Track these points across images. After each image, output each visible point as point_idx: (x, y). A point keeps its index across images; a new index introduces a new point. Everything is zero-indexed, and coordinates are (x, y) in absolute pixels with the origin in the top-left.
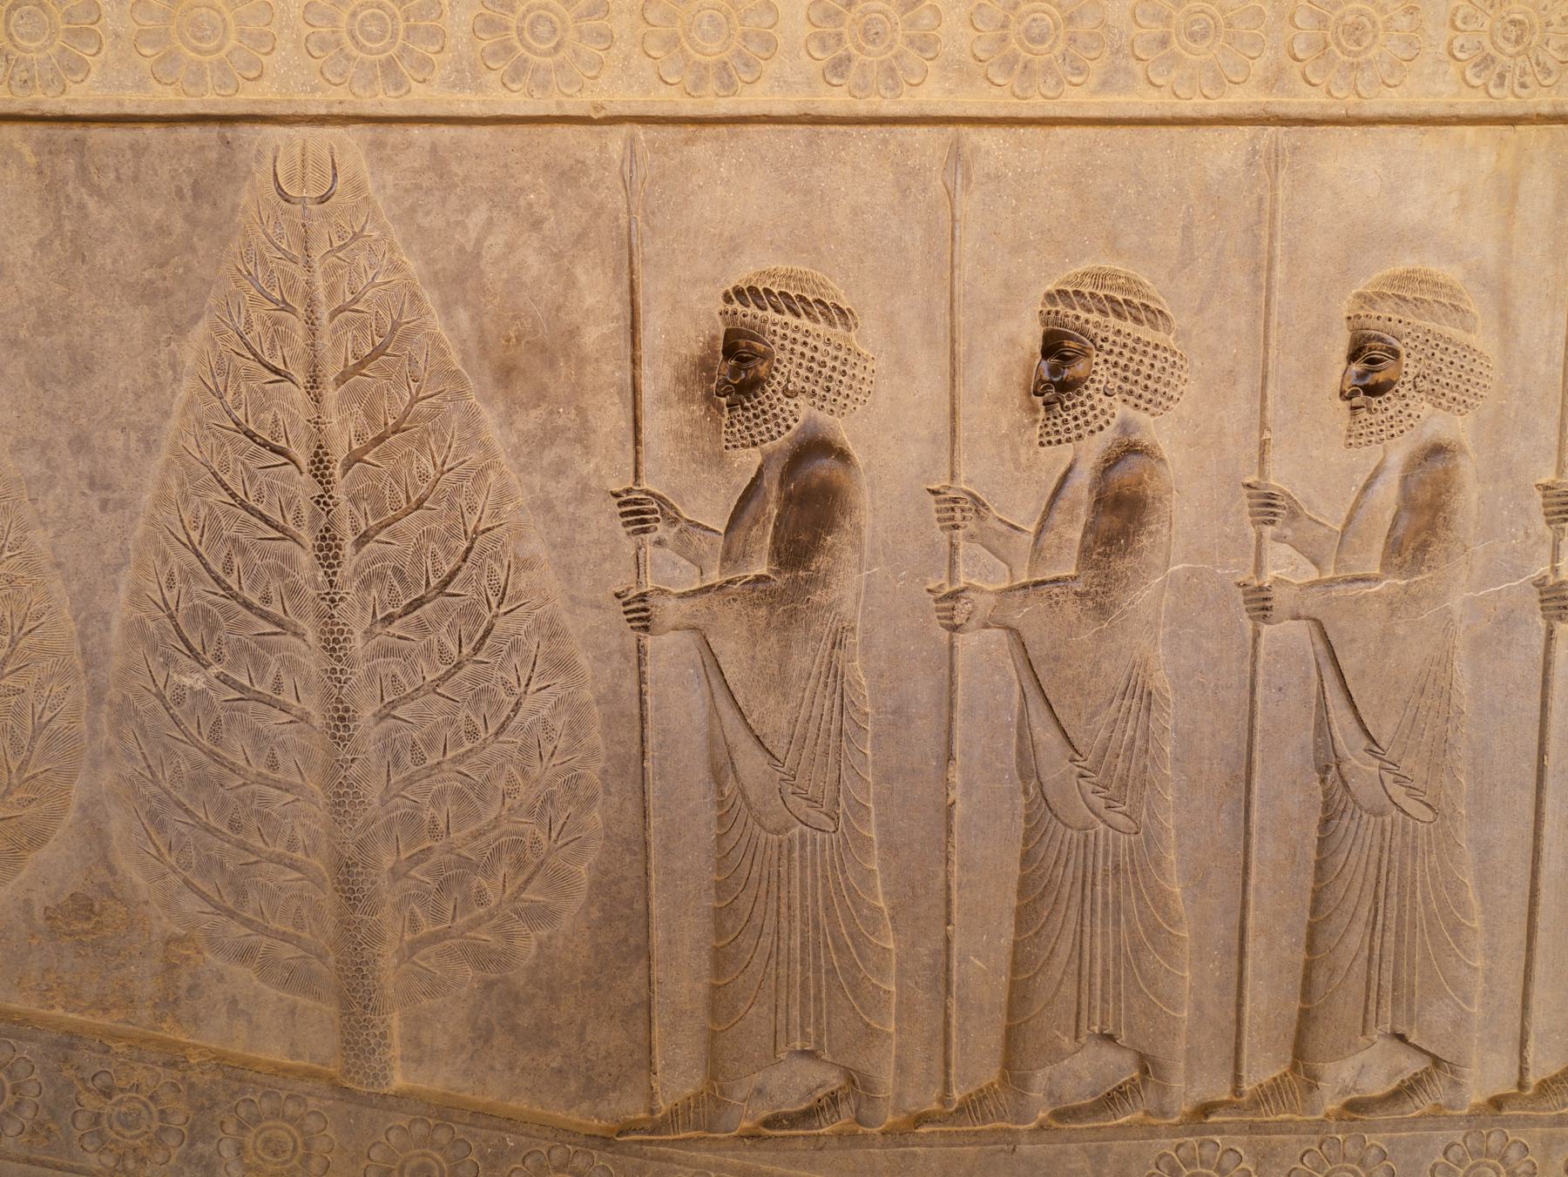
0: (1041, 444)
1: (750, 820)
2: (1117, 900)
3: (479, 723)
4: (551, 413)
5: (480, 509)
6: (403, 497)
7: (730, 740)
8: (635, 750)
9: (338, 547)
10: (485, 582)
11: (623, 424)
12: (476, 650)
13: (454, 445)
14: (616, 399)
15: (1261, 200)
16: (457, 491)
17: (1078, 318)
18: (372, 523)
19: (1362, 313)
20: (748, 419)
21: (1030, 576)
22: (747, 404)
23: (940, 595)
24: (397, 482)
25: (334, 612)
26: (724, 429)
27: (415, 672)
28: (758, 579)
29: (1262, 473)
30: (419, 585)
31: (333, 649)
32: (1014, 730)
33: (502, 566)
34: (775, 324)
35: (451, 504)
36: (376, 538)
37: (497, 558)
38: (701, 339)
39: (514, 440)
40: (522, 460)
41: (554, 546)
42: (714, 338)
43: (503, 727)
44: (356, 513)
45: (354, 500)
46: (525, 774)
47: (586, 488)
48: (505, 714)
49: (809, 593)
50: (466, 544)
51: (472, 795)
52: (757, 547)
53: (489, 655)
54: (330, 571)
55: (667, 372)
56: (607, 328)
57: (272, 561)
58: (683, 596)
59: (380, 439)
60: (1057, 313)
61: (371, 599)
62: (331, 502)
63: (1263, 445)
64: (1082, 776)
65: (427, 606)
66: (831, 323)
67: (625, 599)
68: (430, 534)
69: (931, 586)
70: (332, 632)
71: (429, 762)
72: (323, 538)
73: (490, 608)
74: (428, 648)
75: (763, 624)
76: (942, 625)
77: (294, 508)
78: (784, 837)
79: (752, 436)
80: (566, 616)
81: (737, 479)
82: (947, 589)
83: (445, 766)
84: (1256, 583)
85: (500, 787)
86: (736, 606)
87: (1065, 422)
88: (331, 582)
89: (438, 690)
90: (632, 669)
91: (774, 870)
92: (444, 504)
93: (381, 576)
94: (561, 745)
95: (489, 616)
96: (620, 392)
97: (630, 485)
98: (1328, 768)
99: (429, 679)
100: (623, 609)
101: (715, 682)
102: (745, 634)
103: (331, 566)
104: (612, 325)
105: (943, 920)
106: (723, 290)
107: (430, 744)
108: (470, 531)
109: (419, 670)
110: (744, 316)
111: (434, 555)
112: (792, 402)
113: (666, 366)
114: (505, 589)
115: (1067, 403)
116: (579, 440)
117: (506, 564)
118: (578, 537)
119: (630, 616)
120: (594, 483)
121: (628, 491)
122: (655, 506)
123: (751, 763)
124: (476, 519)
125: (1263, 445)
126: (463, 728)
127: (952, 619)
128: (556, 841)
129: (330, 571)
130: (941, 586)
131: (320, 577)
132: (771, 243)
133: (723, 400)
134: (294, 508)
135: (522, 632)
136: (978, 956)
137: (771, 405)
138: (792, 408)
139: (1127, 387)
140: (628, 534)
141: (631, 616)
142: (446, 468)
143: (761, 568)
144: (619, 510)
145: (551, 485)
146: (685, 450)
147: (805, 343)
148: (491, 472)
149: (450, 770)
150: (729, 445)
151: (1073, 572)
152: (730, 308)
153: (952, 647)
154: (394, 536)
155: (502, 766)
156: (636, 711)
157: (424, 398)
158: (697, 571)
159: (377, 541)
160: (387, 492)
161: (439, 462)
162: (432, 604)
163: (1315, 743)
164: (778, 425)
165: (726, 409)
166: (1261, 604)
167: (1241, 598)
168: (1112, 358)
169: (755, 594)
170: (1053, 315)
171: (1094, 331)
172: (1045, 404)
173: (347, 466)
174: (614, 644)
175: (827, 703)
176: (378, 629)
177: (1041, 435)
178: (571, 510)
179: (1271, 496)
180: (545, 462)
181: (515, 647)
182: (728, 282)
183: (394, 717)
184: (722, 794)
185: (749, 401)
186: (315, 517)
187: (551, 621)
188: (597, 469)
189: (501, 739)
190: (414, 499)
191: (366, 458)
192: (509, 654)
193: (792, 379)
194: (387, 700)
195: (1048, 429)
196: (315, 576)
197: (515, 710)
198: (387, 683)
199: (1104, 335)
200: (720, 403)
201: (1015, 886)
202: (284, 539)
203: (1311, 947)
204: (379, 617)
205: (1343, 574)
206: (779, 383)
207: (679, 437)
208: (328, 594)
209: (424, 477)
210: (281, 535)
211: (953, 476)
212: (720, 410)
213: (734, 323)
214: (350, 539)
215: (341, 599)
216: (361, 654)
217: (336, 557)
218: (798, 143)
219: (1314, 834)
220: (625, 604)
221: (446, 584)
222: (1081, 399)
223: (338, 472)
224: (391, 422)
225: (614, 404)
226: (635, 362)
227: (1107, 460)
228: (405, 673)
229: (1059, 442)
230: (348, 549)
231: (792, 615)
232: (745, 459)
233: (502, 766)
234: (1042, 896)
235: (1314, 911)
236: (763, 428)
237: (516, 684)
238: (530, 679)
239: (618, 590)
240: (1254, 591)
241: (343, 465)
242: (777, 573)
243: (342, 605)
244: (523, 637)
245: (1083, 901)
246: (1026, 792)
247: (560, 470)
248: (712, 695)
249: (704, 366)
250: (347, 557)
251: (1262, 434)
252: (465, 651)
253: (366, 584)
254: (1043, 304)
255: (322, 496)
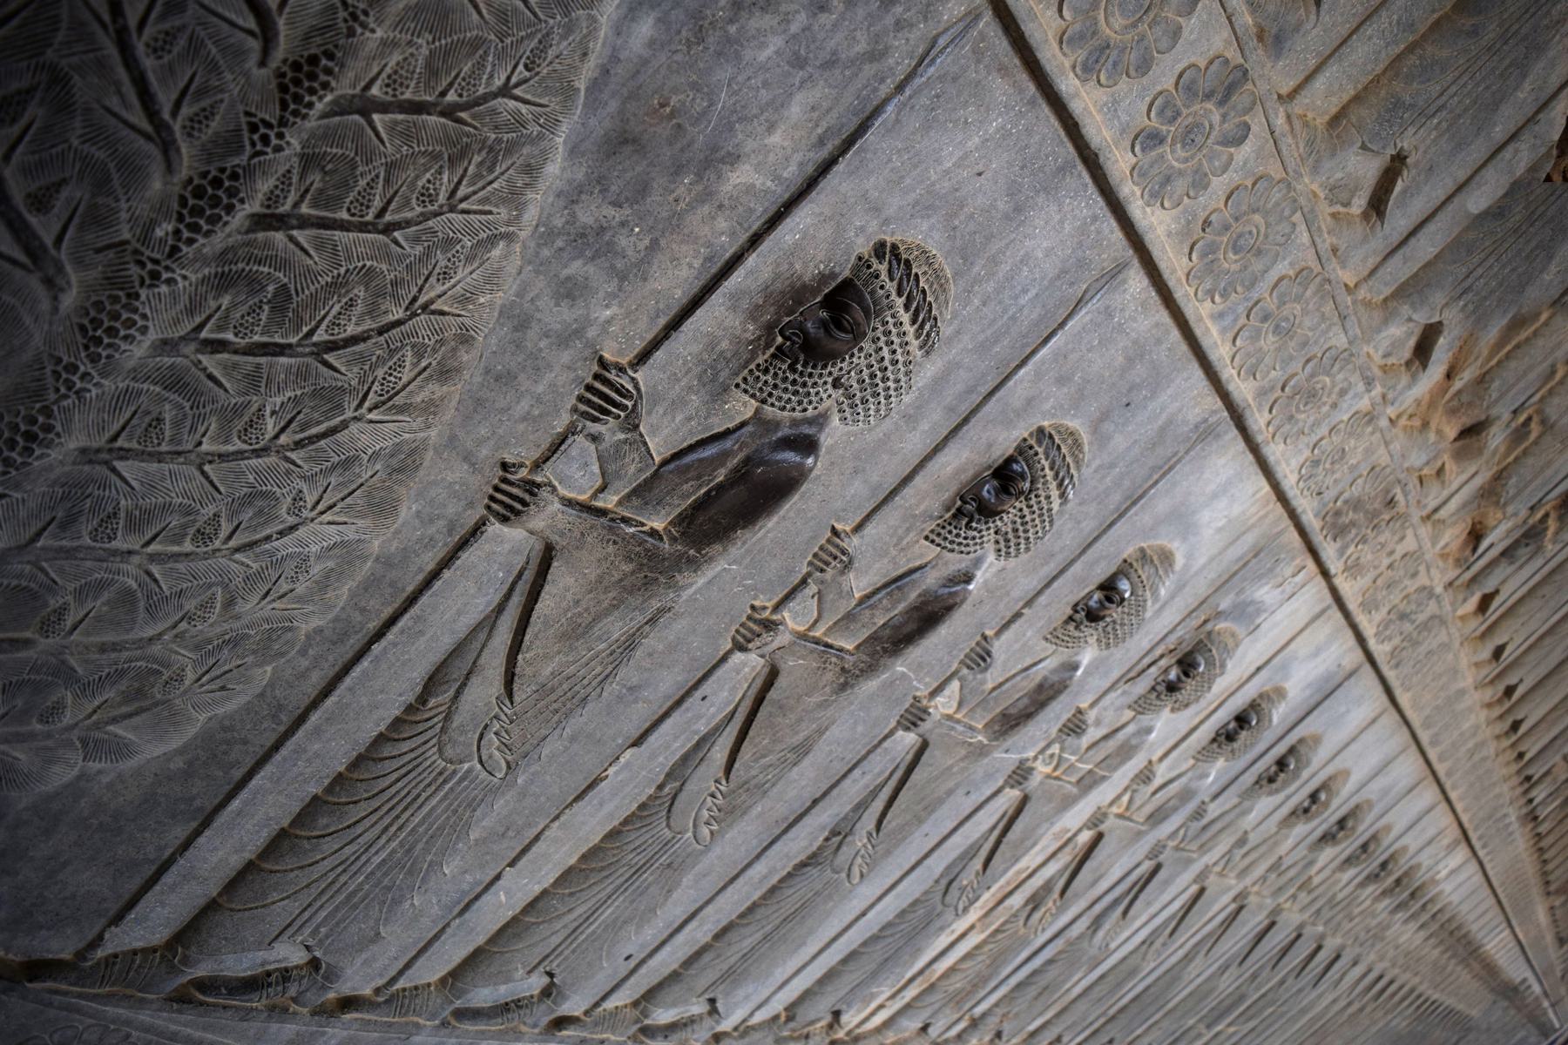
0: (926, 538)
1: (434, 741)
2: (649, 885)
3: (225, 529)
4: (623, 224)
5: (453, 281)
6: (377, 203)
7: (482, 661)
8: (373, 625)
9: (230, 209)
10: (380, 373)
11: (678, 293)
12: (299, 445)
13: (495, 185)
14: (697, 263)
15: (1176, 454)
16: (449, 243)
17: (1043, 469)
18: (305, 209)
19: (1135, 564)
20: (785, 379)
21: (825, 634)
22: (799, 367)
23: (757, 616)
24: (387, 181)
25: (143, 293)
26: (753, 366)
27: (193, 429)
28: (653, 533)
29: (998, 633)
30: (298, 329)
31: (98, 341)
32: (697, 738)
33: (415, 365)
34: (893, 316)
35: (428, 254)
36: (295, 233)
37: (419, 355)
38: (822, 267)
39: (558, 222)
40: (546, 252)
41: (487, 371)
42: (833, 275)
43: (251, 545)
44: (295, 179)
45: (309, 161)
46: (229, 603)
47: (578, 333)
48: (268, 532)
49: (680, 572)
50: (399, 314)
51: (142, 604)
52: (676, 502)
53: (308, 459)
54: (186, 234)
55: (766, 274)
56: (761, 181)
57: (101, 155)
58: (569, 503)
59: (418, 108)
60: (1036, 454)
61: (213, 304)
62: (274, 141)
63: (1018, 615)
64: (713, 796)
65: (283, 360)
66: (921, 348)
67: (509, 476)
68: (368, 275)
69: (757, 603)
70: (115, 316)
71: (115, 544)
72: (217, 183)
73: (360, 405)
74: (237, 411)
75: (617, 576)
76: (733, 639)
77: (205, 103)
78: (451, 767)
79: (770, 395)
80: (430, 454)
81: (714, 420)
82: (766, 614)
83: (136, 559)
84: (925, 702)
85: (187, 608)
86: (611, 548)
87: (958, 535)
88: (175, 250)
89: (207, 468)
90: (445, 545)
91: (415, 792)
92: (419, 249)
93: (254, 284)
94: (300, 589)
95: (349, 414)
96: (709, 259)
97: (624, 361)
98: (839, 833)
99: (205, 447)
100: (496, 481)
101: (517, 600)
102: (593, 577)
103: (194, 228)
104: (769, 183)
105: (508, 861)
106: (883, 236)
107: (134, 525)
108: (422, 300)
109: (201, 429)
110: (882, 287)
111: (351, 304)
112: (830, 391)
113: (770, 269)
114: (396, 394)
115: (974, 525)
116: (623, 277)
117: (423, 364)
118: (522, 377)
119: (499, 496)
120: (591, 333)
121: (621, 370)
122: (629, 404)
123: (484, 690)
124: (440, 289)
125: (1018, 615)
126: (198, 525)
127: (749, 641)
128: (203, 685)
129: (186, 234)
130: (765, 608)
131: (163, 230)
132: (954, 228)
133: (779, 340)
134: (205, 103)
135: (370, 452)
136: (506, 893)
137: (816, 383)
138: (825, 396)
139: (1010, 536)
140: (575, 410)
141: (499, 496)
142: (463, 206)
143: (658, 525)
144: (589, 380)
145: (545, 302)
146: (701, 361)
147: (894, 352)
148: (502, 244)
149: (139, 566)
150: (743, 386)
151: (850, 647)
152: (876, 265)
153: (724, 659)
154: (319, 247)
155: (210, 586)
156: (410, 589)
157: (517, 98)
158: (599, 483)
159: (292, 239)
160: (362, 183)
161: (461, 193)
162: (293, 360)
163: (847, 815)
164: (800, 403)
165: (772, 350)
166: (914, 719)
167: (907, 705)
168: (1026, 512)
169: (638, 549)
170: (1032, 452)
171: (1040, 486)
172: (959, 510)
173: (339, 108)
174: (451, 510)
175: (599, 669)
176: (190, 349)
177: (932, 531)
178: (542, 345)
179: (989, 654)
180: (566, 272)
181: (347, 464)
182: (893, 234)
183: (114, 470)
184: (424, 703)
185: (803, 366)
186: (230, 142)
187: (413, 452)
188: (609, 322)
189: (237, 556)
190: (388, 217)
191: (376, 117)
192: (334, 467)
193: (853, 373)
194: (120, 443)
195: (942, 532)
196: (152, 224)
197: (282, 534)
198: (140, 423)
199: (1040, 492)
200: (774, 339)
201: (584, 849)
202: (148, 137)
203: (718, 936)
204: (204, 334)
205: (966, 720)
206: (841, 369)
207: (711, 345)
208: (156, 262)
209: (427, 196)
210: (148, 128)
211: (858, 528)
212: (767, 346)
213: (866, 284)
214: (254, 206)
215: (170, 281)
216: (131, 364)
217: (214, 219)
218: (1056, 160)
219: (789, 869)
220: (504, 480)
221: (332, 346)
222: (984, 527)
223: (319, 106)
224: (451, 97)
225: (690, 266)
226: (755, 241)
227: (950, 580)
228: (177, 424)
229: (938, 545)
230: (238, 219)
231: (648, 583)
232: (739, 407)
233: (210, 586)
234: (603, 869)
235: (742, 916)
236: (786, 396)
237: (309, 506)
238: (330, 507)
239: (510, 459)
240: (919, 709)
241: (335, 102)
242: (674, 540)
243: (164, 289)
244: (366, 458)
245: (627, 881)
246: (660, 787)
247: (570, 291)
248: (500, 609)
249: (798, 293)
250: (227, 229)
251: (1023, 608)
252: (283, 439)
253: (223, 282)
254: (1031, 435)
255: (269, 125)
